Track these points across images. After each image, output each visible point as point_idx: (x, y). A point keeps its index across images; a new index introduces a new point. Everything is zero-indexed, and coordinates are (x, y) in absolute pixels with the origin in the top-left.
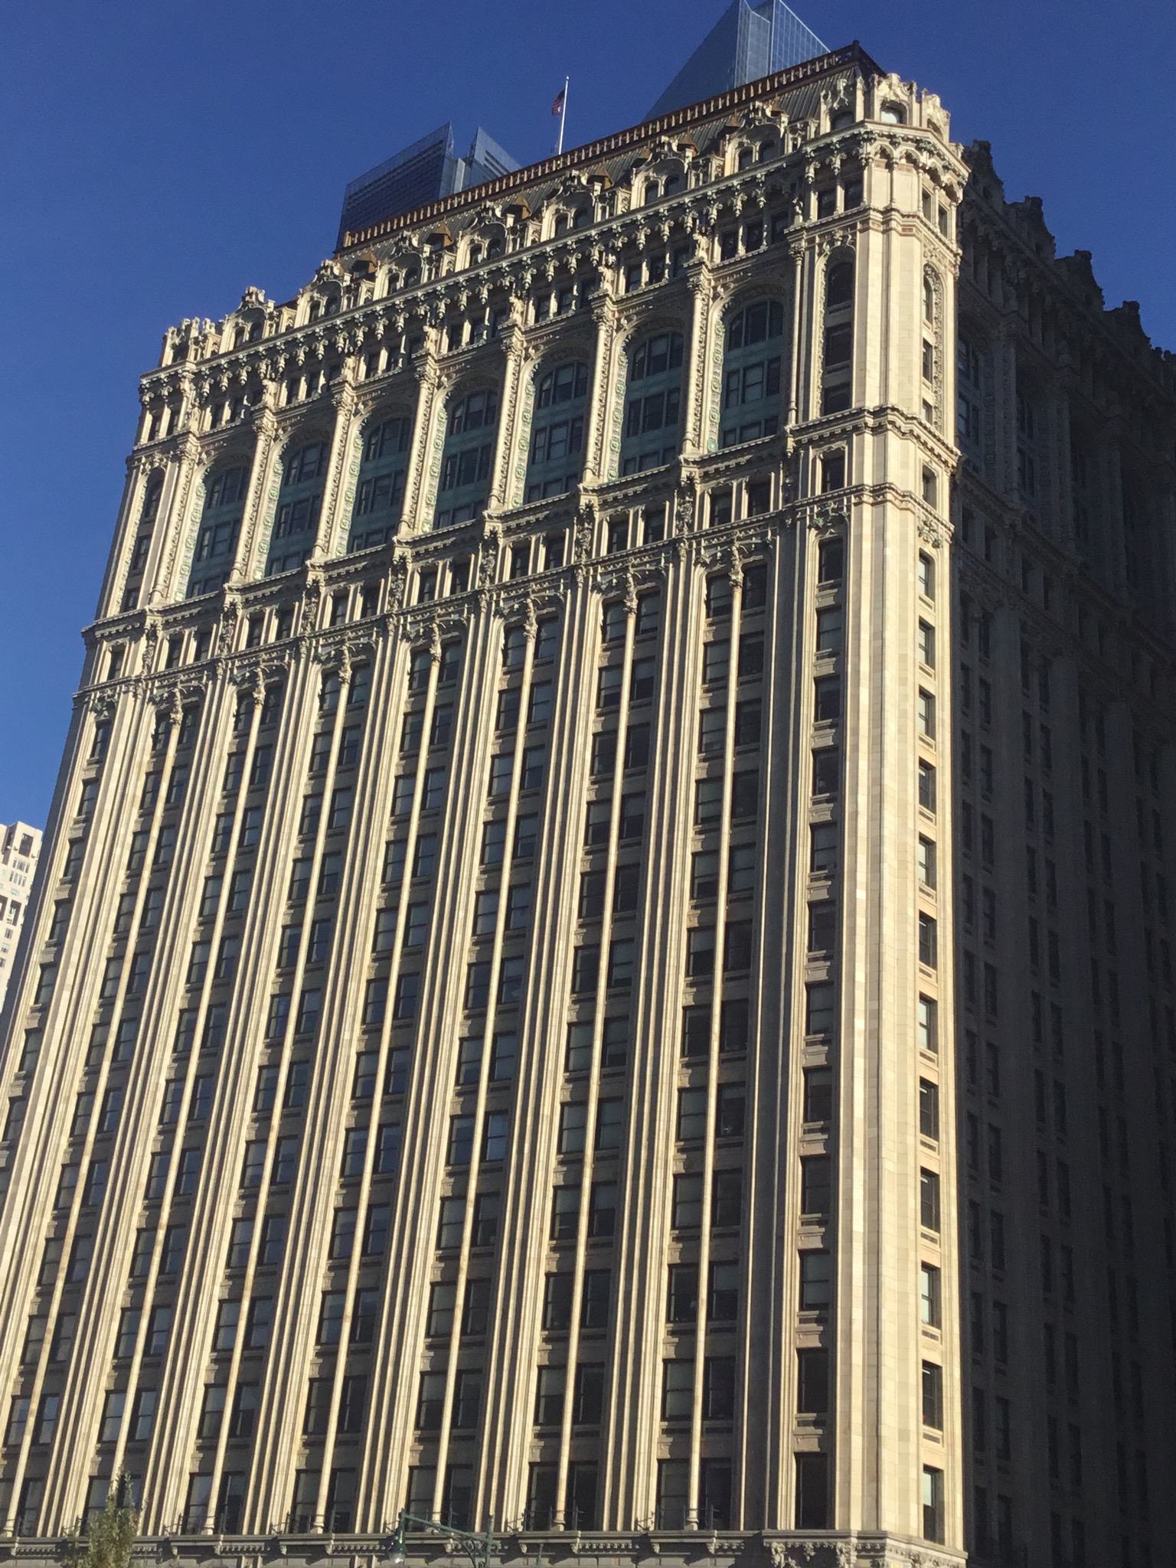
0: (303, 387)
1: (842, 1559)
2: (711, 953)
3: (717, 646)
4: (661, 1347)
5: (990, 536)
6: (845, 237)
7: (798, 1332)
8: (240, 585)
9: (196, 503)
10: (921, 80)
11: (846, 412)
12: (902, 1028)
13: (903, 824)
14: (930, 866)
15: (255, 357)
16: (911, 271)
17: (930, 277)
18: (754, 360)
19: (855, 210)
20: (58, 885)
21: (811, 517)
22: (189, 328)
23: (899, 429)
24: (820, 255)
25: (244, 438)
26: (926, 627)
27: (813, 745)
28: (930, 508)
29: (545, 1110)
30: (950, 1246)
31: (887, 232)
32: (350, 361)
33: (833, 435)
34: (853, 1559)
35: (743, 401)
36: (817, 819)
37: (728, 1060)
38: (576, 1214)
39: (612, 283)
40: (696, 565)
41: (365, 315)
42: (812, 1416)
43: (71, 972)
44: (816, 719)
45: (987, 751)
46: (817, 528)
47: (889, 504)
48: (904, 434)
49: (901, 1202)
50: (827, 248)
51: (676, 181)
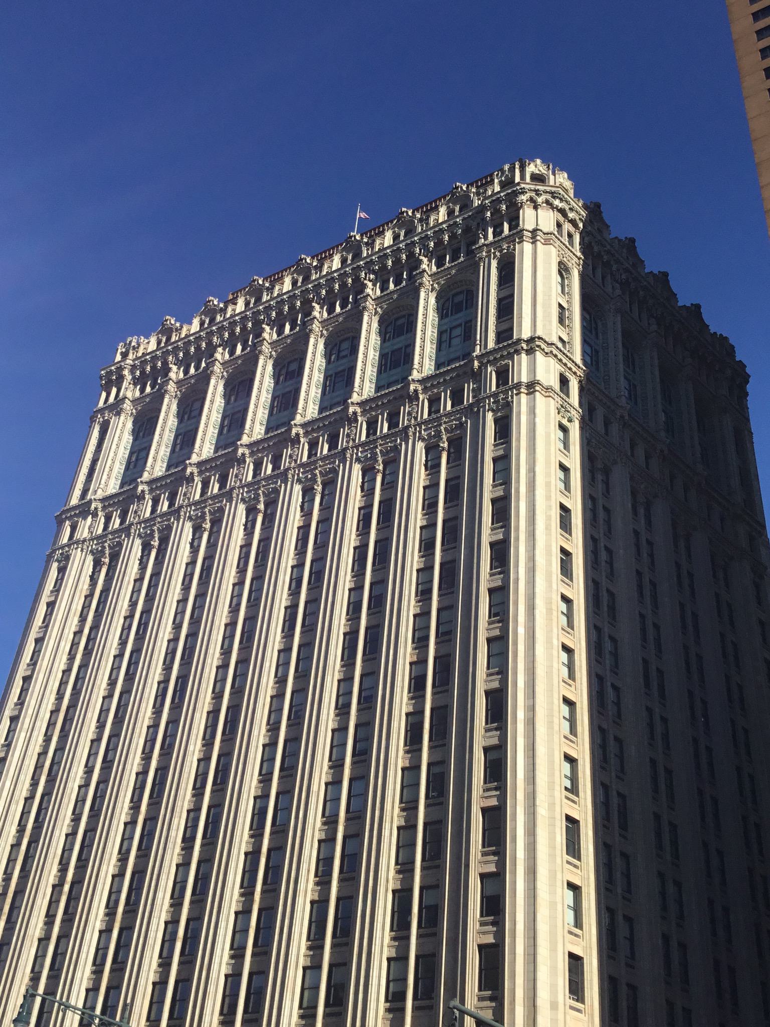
2: (424, 677)
3: (431, 488)
4: (386, 949)
5: (607, 423)
6: (509, 247)
8: (148, 480)
9: (127, 439)
10: (557, 162)
11: (510, 342)
12: (550, 715)
13: (550, 586)
14: (569, 615)
15: (167, 353)
16: (550, 263)
17: (563, 270)
18: (455, 324)
19: (515, 231)
20: (25, 667)
21: (489, 404)
22: (131, 342)
23: (543, 350)
26: (564, 468)
27: (490, 540)
28: (565, 397)
29: (315, 787)
30: (588, 871)
32: (220, 350)
33: (502, 356)
36: (493, 585)
37: (436, 747)
39: (372, 290)
41: (230, 323)
42: (488, 993)
43: (27, 720)
45: (609, 551)
46: (493, 411)
48: (547, 353)
49: (551, 838)
50: (498, 254)
51: (410, 232)
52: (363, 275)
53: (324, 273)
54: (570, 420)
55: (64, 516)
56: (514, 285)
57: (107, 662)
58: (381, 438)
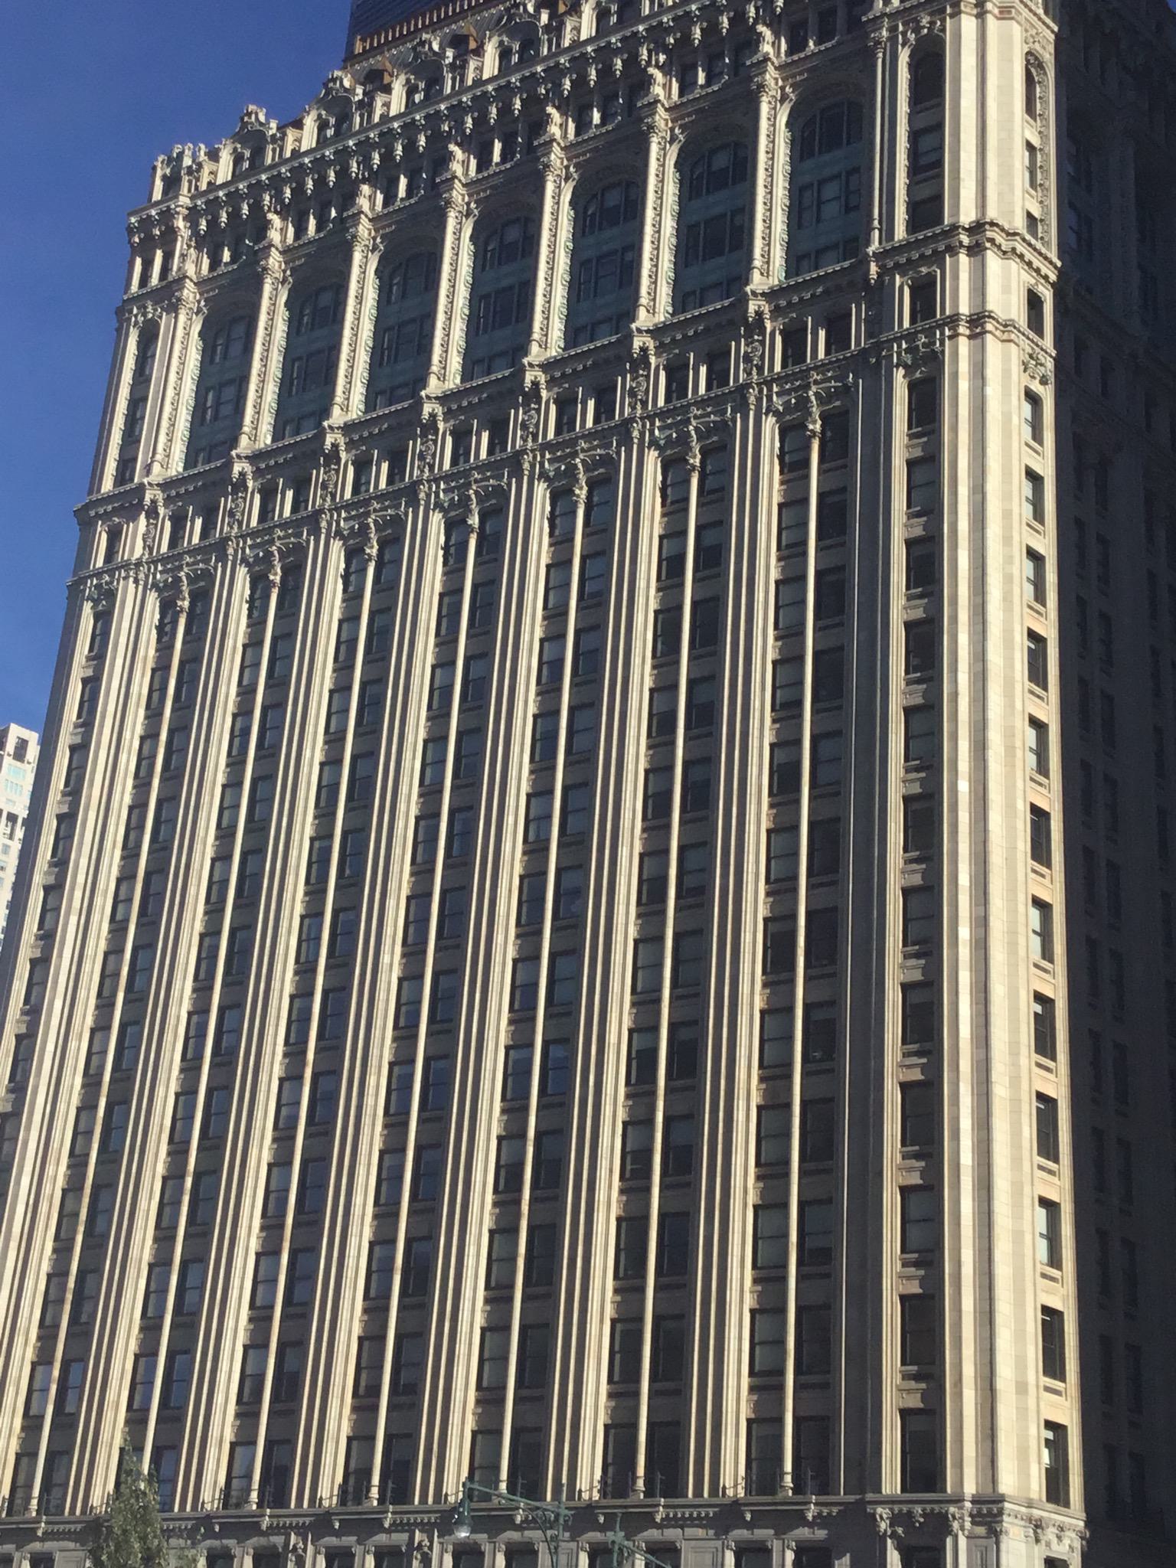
0: (312, 223)
1: (956, 1525)
7: (901, 1277)
8: (249, 452)
12: (1012, 933)
13: (1010, 705)
16: (1011, 61)
18: (827, 172)
20: (59, 797)
21: (899, 354)
22: (181, 155)
23: (999, 247)
24: (903, 46)
25: (250, 279)
26: (1033, 477)
28: (1036, 338)
29: (612, 1037)
31: (981, 16)
32: (366, 189)
34: (968, 1525)
35: (818, 221)
38: (650, 1152)
39: (663, 89)
40: (767, 414)
41: (381, 135)
43: (78, 894)
44: (908, 588)
47: (989, 337)
48: (1005, 253)
50: (912, 37)
53: (567, 43)
54: (1044, 381)
55: (92, 513)
56: (942, 105)
58: (696, 404)
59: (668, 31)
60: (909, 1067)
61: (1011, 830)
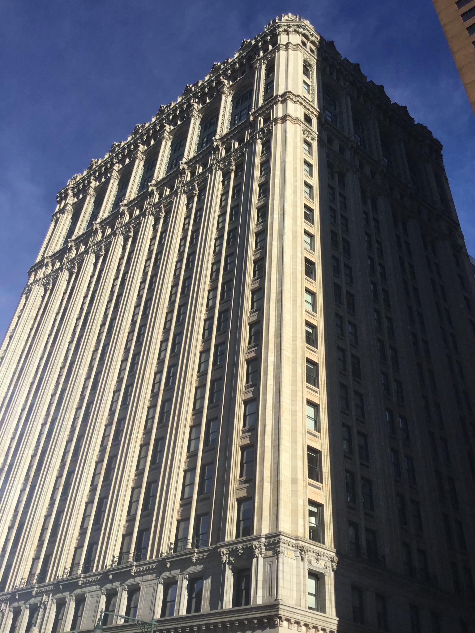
1: (257, 552)
23: (292, 100)
34: (263, 551)
47: (288, 122)
48: (295, 102)
52: (192, 101)
57: (43, 338)
59: (197, 93)
60: (249, 353)
61: (295, 264)
